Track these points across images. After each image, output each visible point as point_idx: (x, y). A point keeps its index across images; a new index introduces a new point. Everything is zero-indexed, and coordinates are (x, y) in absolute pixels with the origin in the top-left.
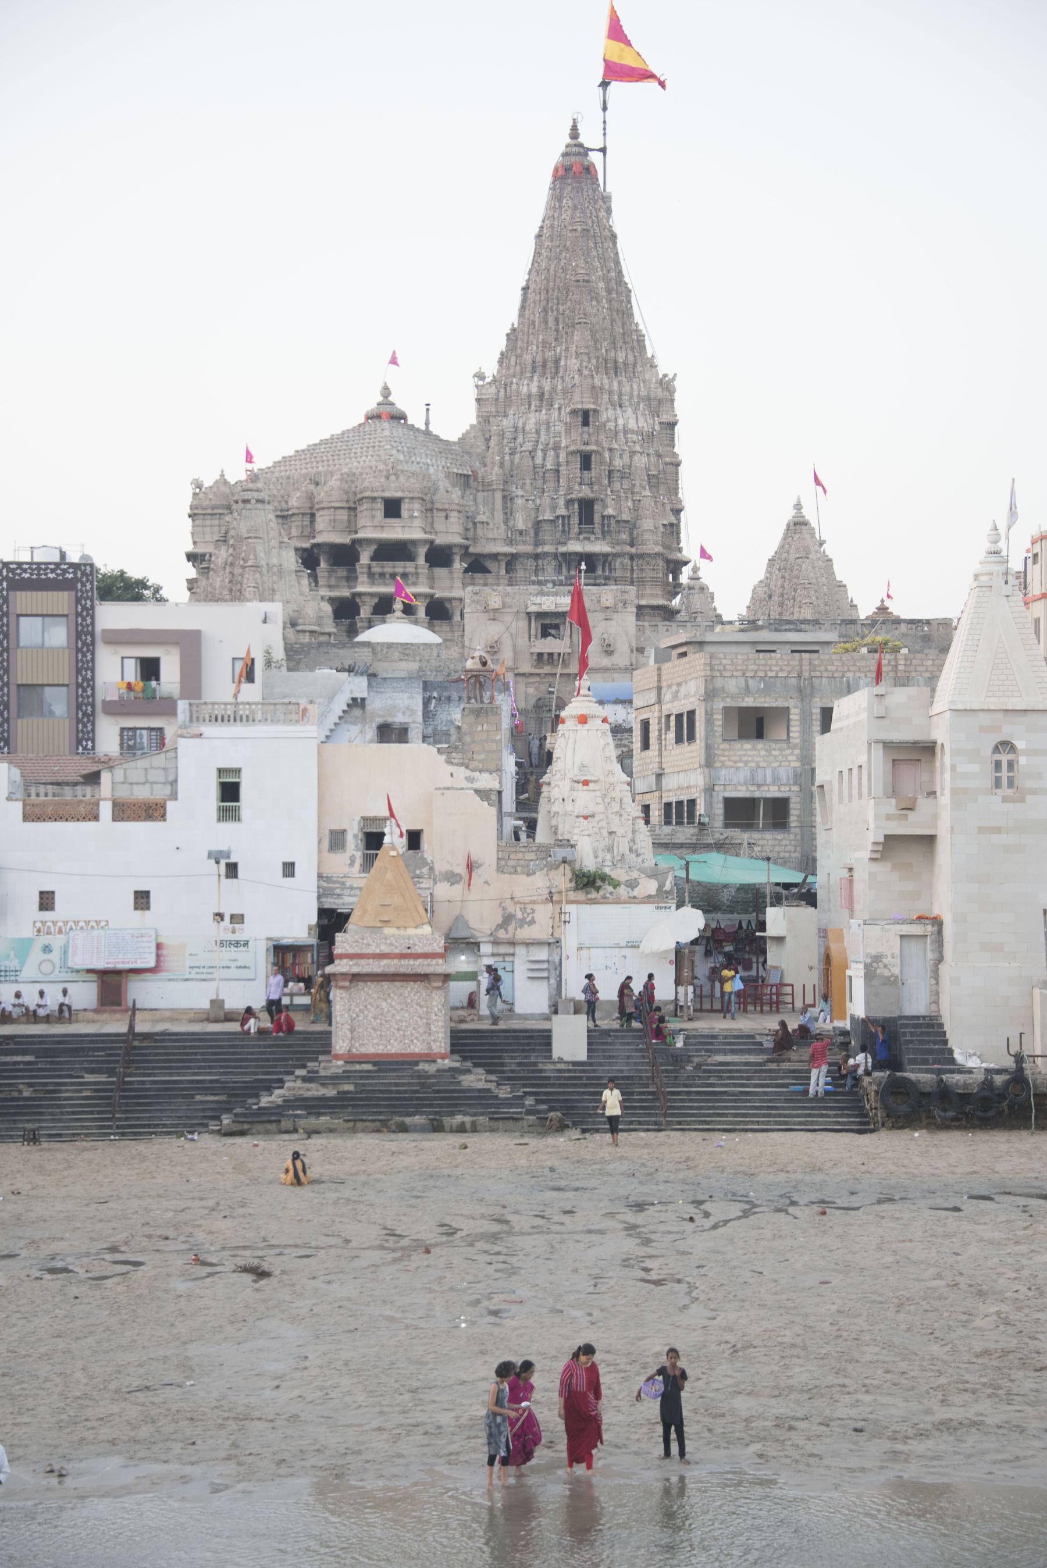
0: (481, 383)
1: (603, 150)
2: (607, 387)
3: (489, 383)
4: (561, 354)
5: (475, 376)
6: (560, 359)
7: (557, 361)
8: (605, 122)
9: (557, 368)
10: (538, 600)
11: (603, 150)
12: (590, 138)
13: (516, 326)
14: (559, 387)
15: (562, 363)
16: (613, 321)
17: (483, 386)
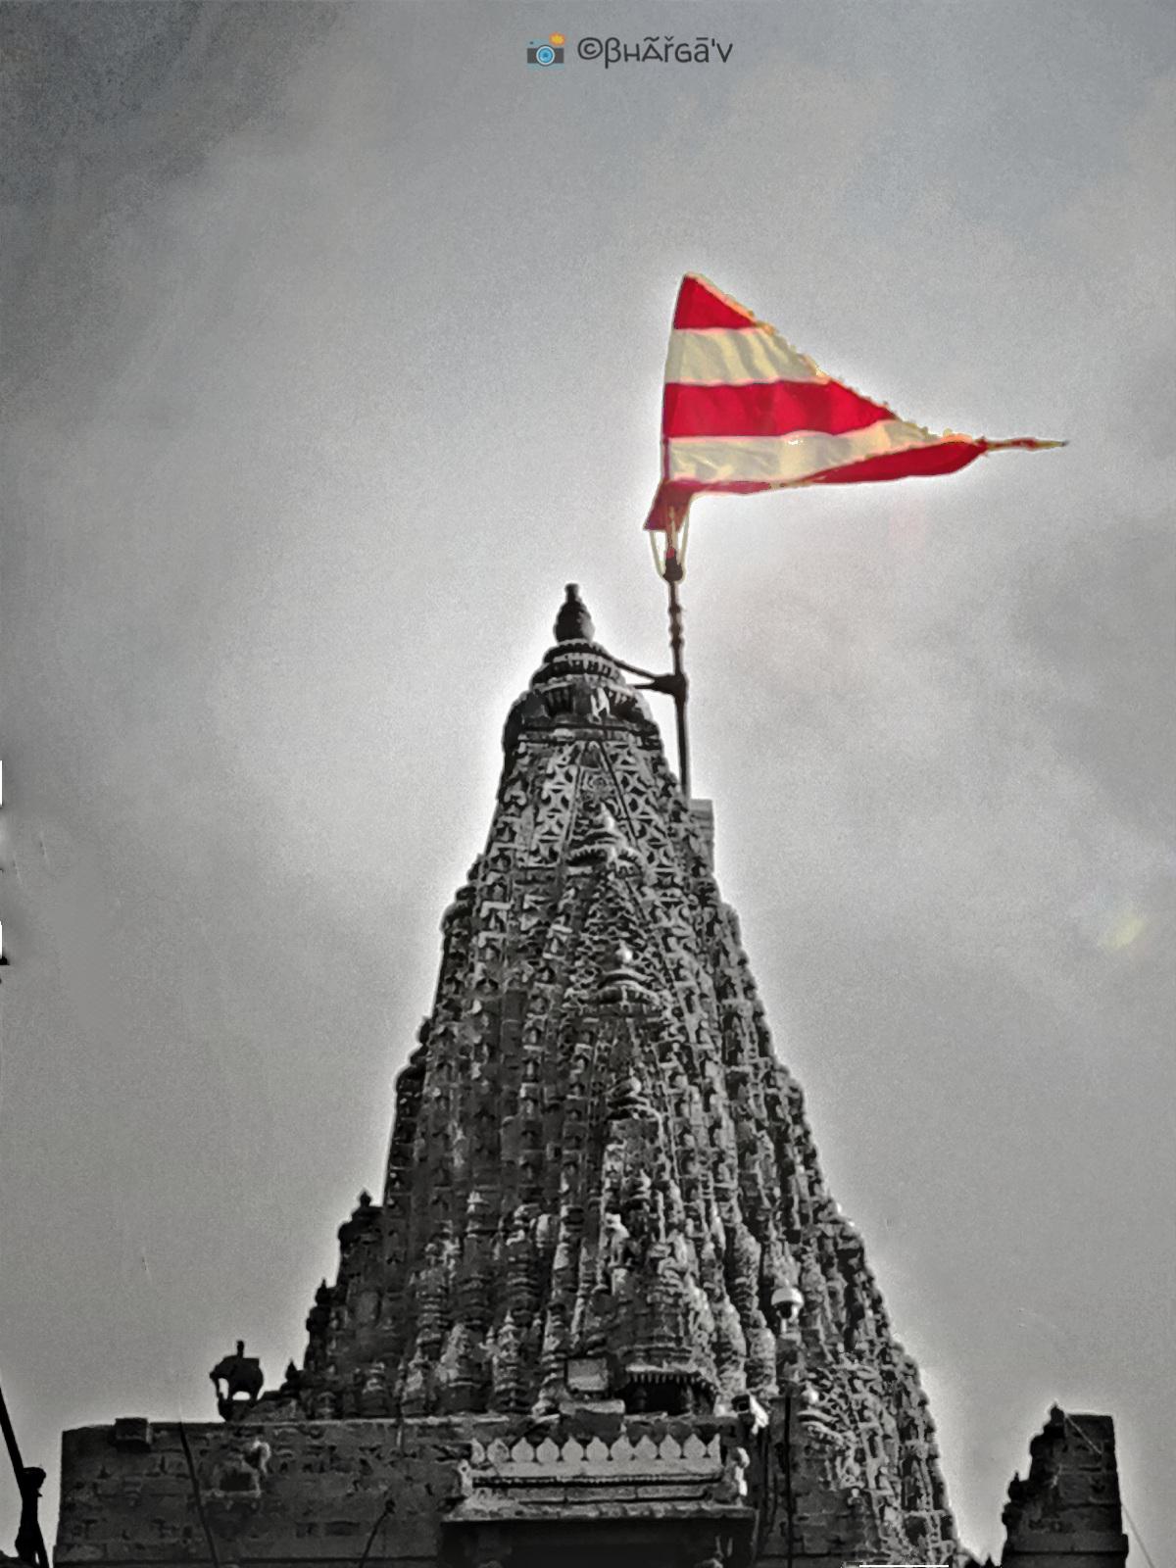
0: (242, 1396)
1: (673, 685)
2: (739, 1343)
3: (277, 1398)
4: (553, 1230)
5: (215, 1376)
6: (550, 1254)
7: (539, 1264)
8: (675, 609)
9: (540, 1290)
10: (523, 1461)
11: (673, 685)
12: (629, 640)
13: (377, 1201)
14: (550, 1343)
15: (560, 1261)
16: (747, 1148)
17: (252, 1403)
